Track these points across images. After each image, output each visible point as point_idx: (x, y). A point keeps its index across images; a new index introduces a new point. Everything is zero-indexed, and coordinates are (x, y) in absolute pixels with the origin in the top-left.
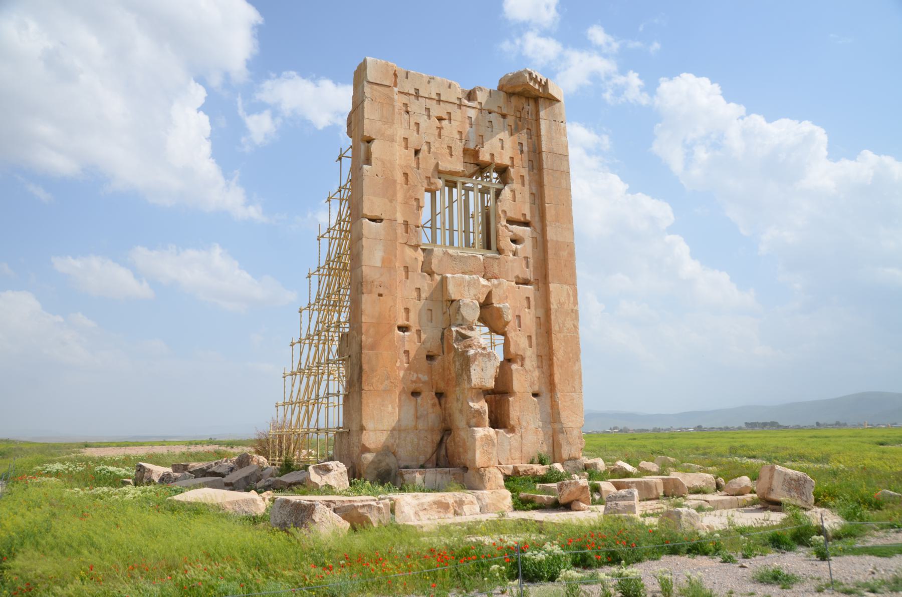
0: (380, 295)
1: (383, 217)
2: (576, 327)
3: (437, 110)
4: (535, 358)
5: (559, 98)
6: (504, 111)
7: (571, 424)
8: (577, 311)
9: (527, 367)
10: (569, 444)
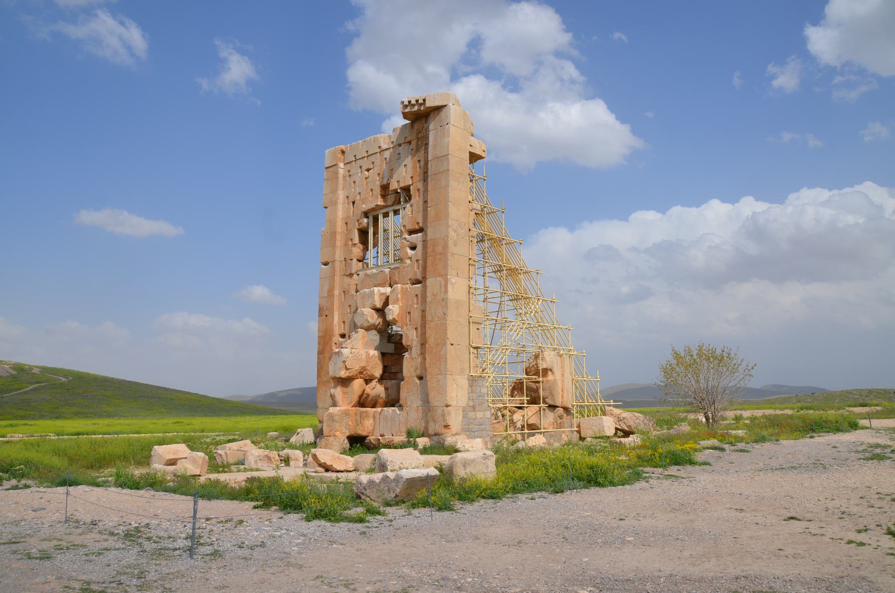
2: (445, 314)
3: (366, 164)
4: (419, 345)
7: (436, 404)
10: (434, 421)
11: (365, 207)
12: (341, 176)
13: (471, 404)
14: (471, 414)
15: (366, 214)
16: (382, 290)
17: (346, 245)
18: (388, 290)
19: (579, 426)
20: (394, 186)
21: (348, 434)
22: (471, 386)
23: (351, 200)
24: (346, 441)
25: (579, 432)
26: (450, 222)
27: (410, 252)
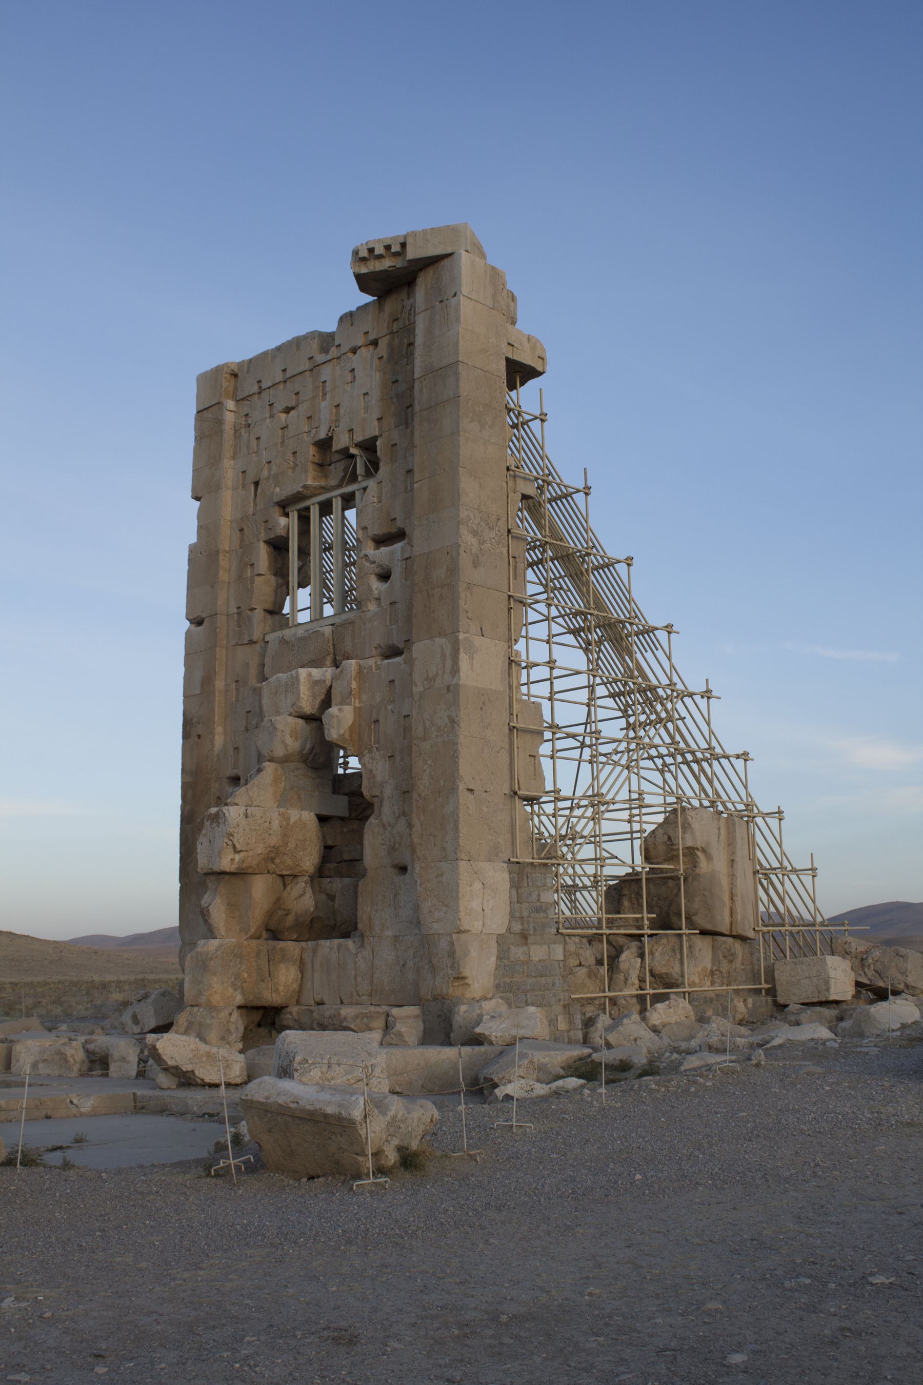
0: (199, 736)
1: (204, 616)
2: (453, 721)
5: (449, 251)
6: (372, 337)
8: (457, 686)
9: (385, 821)
11: (280, 493)
12: (228, 428)
13: (517, 927)
14: (518, 952)
15: (284, 506)
16: (316, 673)
17: (240, 578)
18: (326, 673)
19: (771, 978)
20: (341, 441)
21: (239, 999)
22: (516, 885)
23: (251, 478)
24: (236, 1016)
25: (772, 992)
26: (463, 514)
27: (376, 585)
